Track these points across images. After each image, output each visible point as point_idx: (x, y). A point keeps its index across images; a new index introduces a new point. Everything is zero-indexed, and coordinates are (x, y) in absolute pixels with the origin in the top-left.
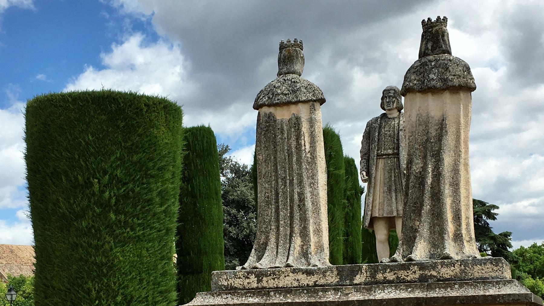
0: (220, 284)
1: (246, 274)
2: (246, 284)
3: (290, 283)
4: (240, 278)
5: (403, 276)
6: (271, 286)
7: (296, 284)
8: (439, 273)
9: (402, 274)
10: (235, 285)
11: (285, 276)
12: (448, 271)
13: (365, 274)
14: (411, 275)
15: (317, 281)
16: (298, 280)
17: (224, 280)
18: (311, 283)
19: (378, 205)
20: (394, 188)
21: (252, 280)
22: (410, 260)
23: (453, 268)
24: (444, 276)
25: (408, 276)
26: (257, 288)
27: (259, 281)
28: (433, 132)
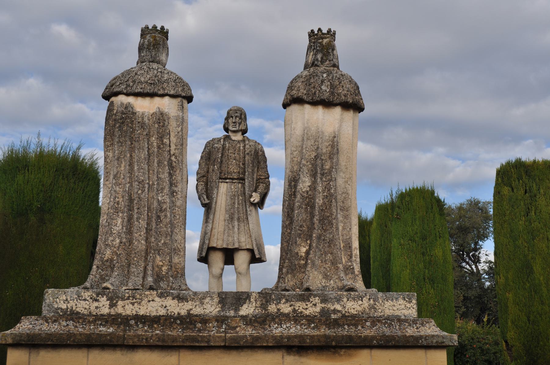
0: (56, 306)
1: (95, 296)
2: (93, 308)
3: (154, 310)
4: (85, 300)
5: (301, 308)
6: (129, 312)
7: (162, 312)
8: (345, 307)
9: (300, 306)
10: (78, 310)
11: (149, 301)
12: (355, 306)
13: (254, 304)
14: (310, 309)
15: (191, 309)
16: (166, 307)
17: (62, 302)
18: (183, 312)
20: (236, 216)
21: (103, 303)
22: (308, 289)
23: (360, 302)
24: (350, 311)
25: (307, 309)
26: (109, 315)
27: (112, 306)
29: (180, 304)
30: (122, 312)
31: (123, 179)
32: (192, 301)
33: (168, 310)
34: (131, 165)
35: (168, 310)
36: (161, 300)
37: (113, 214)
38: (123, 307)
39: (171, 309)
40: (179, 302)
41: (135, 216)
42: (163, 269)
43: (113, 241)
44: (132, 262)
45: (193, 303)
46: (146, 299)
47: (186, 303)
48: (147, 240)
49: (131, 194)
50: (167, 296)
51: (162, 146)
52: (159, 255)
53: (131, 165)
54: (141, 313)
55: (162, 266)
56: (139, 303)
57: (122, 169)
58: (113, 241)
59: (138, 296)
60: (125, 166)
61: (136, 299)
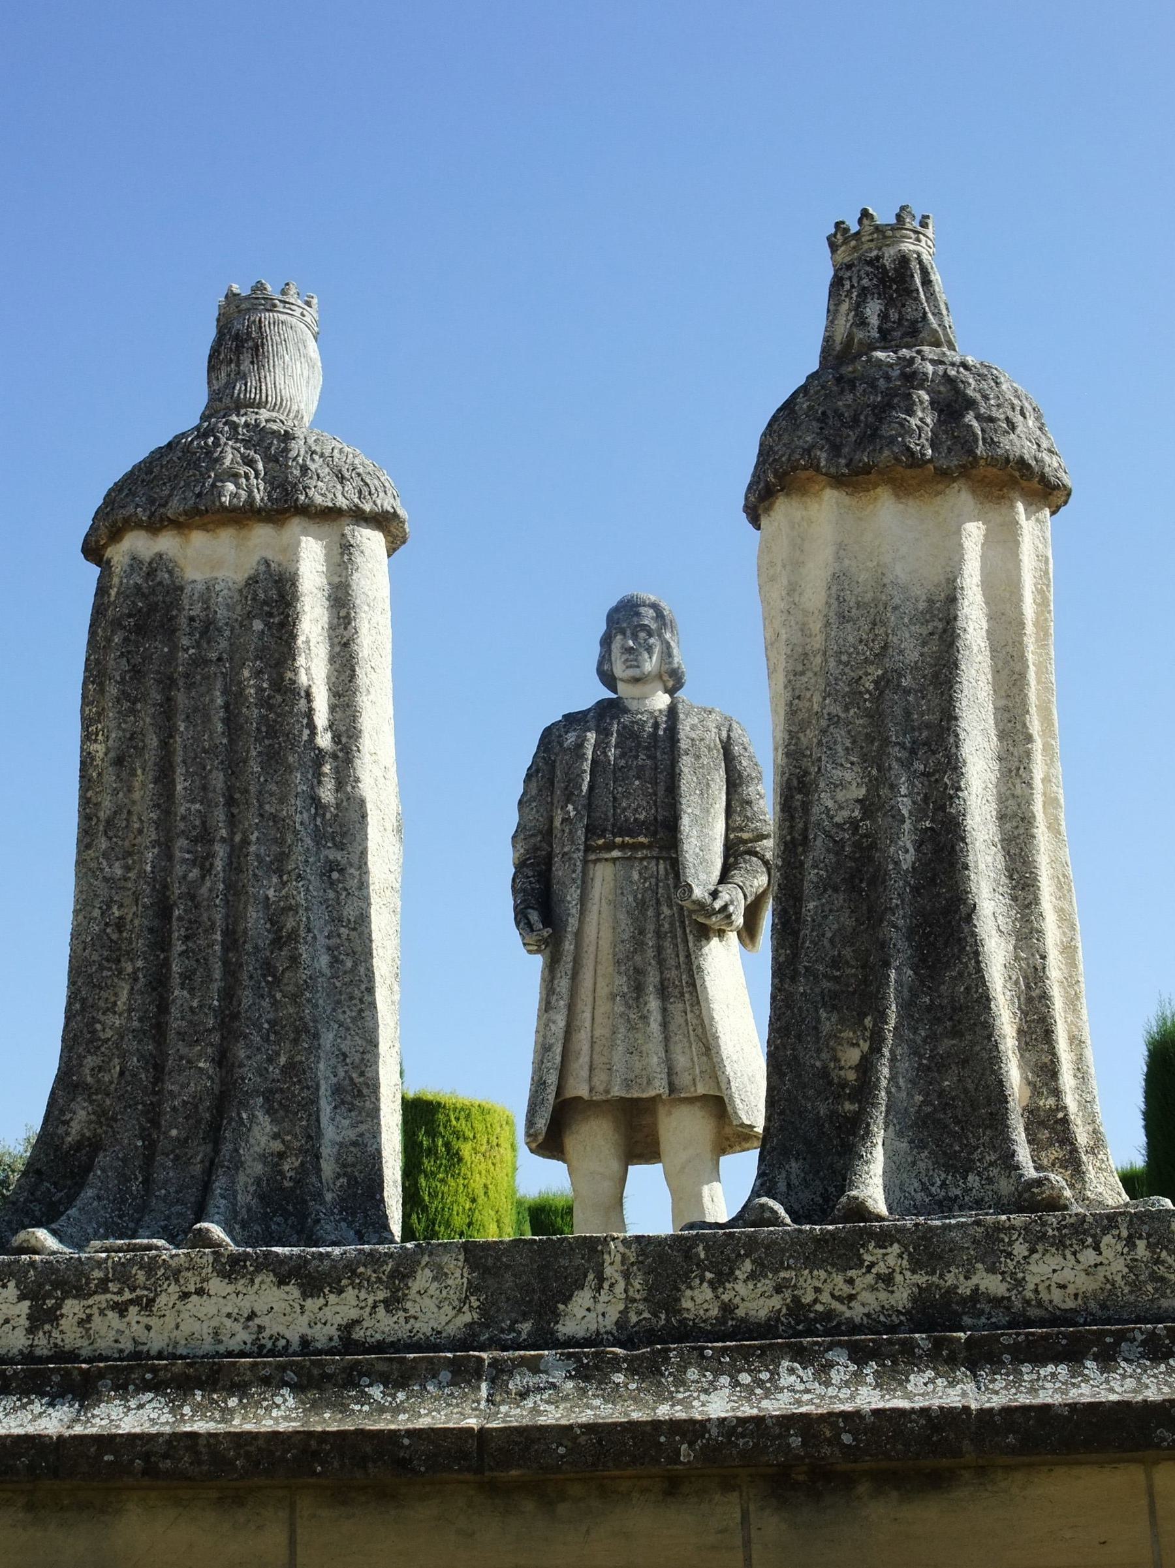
6: (104, 1344)
7: (240, 1337)
11: (185, 1296)
15: (357, 1322)
16: (252, 1316)
18: (322, 1335)
19: (585, 1048)
28: (909, 648)
29: (309, 1303)
30: (79, 1343)
31: (140, 831)
32: (360, 1287)
33: (261, 1328)
34: (164, 776)
35: (261, 1328)
36: (230, 1288)
37: (101, 968)
38: (81, 1323)
39: (273, 1326)
40: (305, 1296)
41: (176, 968)
42: (286, 1167)
43: (100, 1069)
44: (163, 1144)
45: (363, 1295)
46: (173, 1288)
47: (332, 1298)
48: (222, 1059)
49: (165, 886)
50: (258, 1270)
51: (279, 698)
52: (270, 1111)
53: (164, 776)
54: (156, 1342)
55: (281, 1155)
56: (147, 1305)
57: (137, 795)
58: (100, 1069)
59: (141, 1276)
60: (143, 785)
61: (133, 1289)
